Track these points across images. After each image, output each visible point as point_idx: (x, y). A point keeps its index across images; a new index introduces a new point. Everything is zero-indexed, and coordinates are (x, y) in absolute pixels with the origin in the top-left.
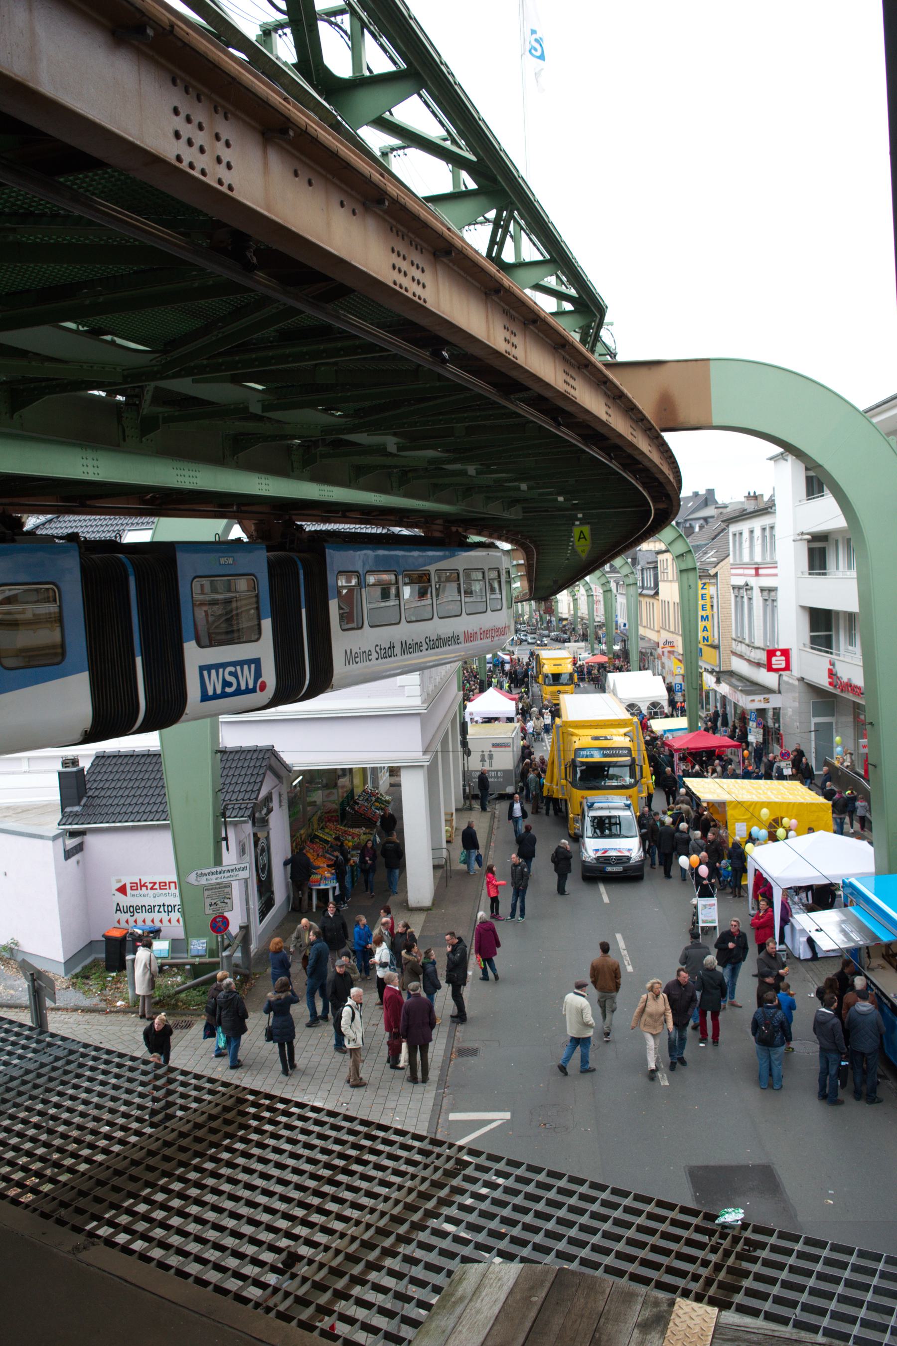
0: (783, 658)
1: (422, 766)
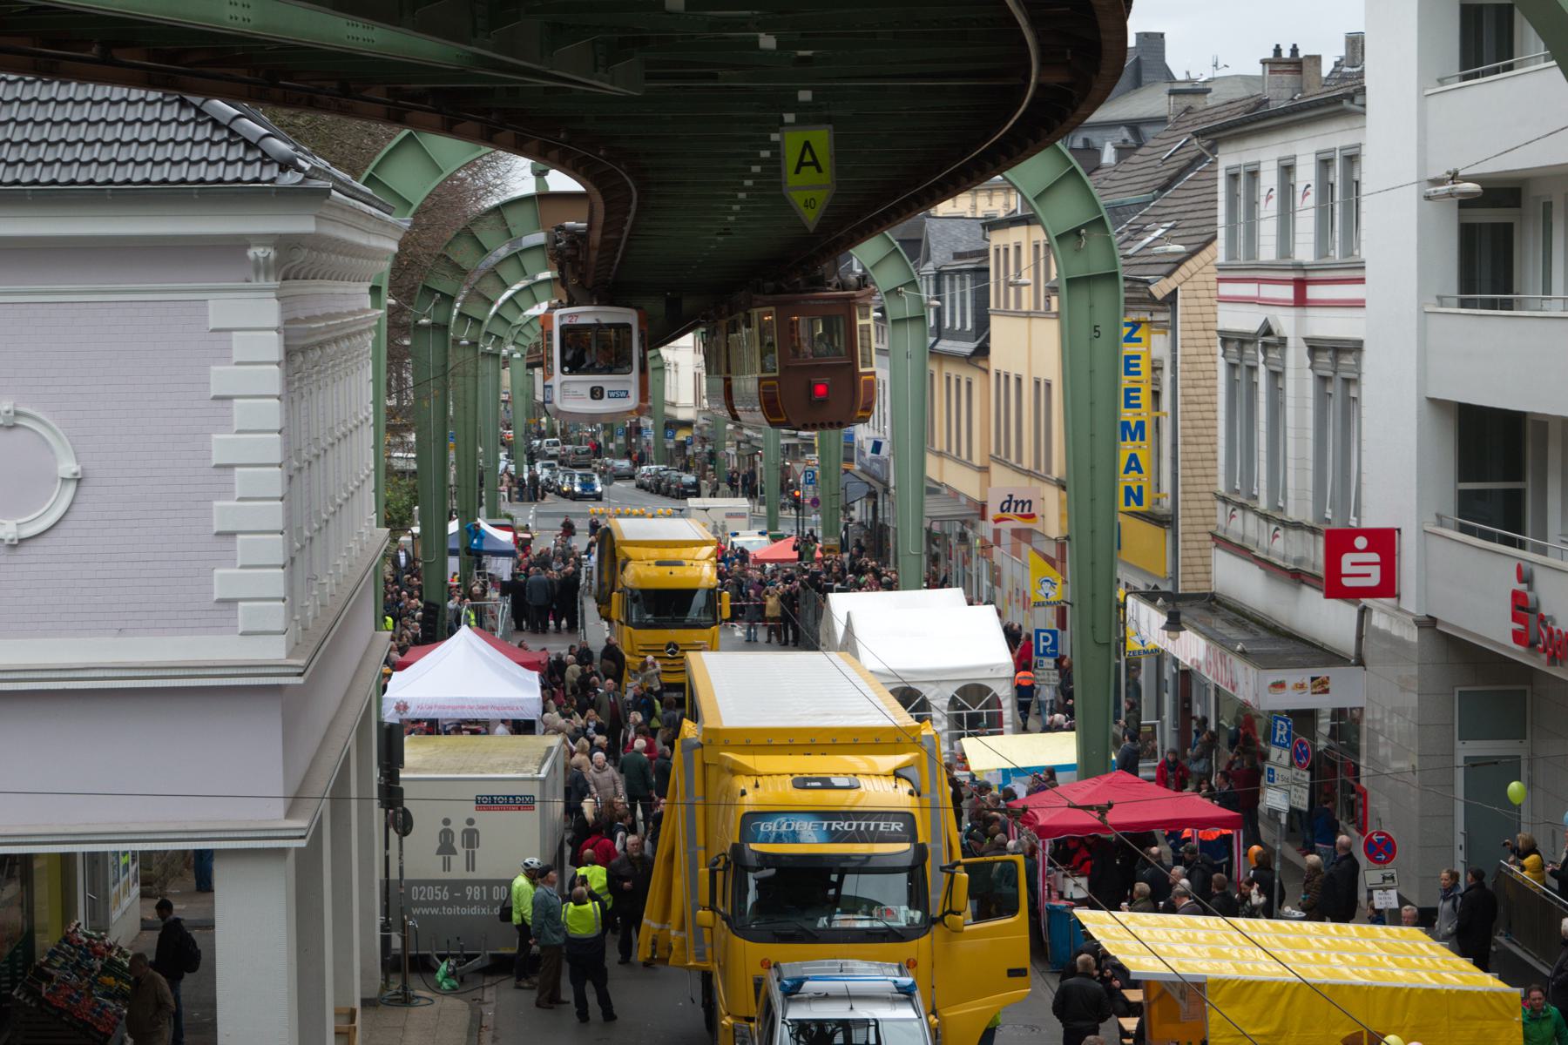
0: (1375, 557)
1: (282, 852)
